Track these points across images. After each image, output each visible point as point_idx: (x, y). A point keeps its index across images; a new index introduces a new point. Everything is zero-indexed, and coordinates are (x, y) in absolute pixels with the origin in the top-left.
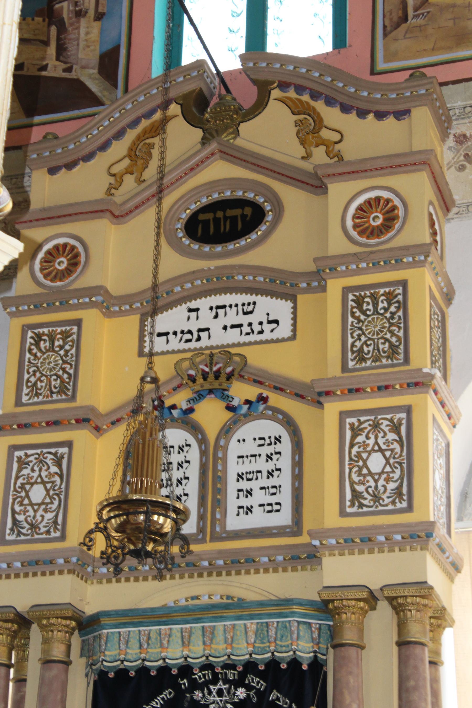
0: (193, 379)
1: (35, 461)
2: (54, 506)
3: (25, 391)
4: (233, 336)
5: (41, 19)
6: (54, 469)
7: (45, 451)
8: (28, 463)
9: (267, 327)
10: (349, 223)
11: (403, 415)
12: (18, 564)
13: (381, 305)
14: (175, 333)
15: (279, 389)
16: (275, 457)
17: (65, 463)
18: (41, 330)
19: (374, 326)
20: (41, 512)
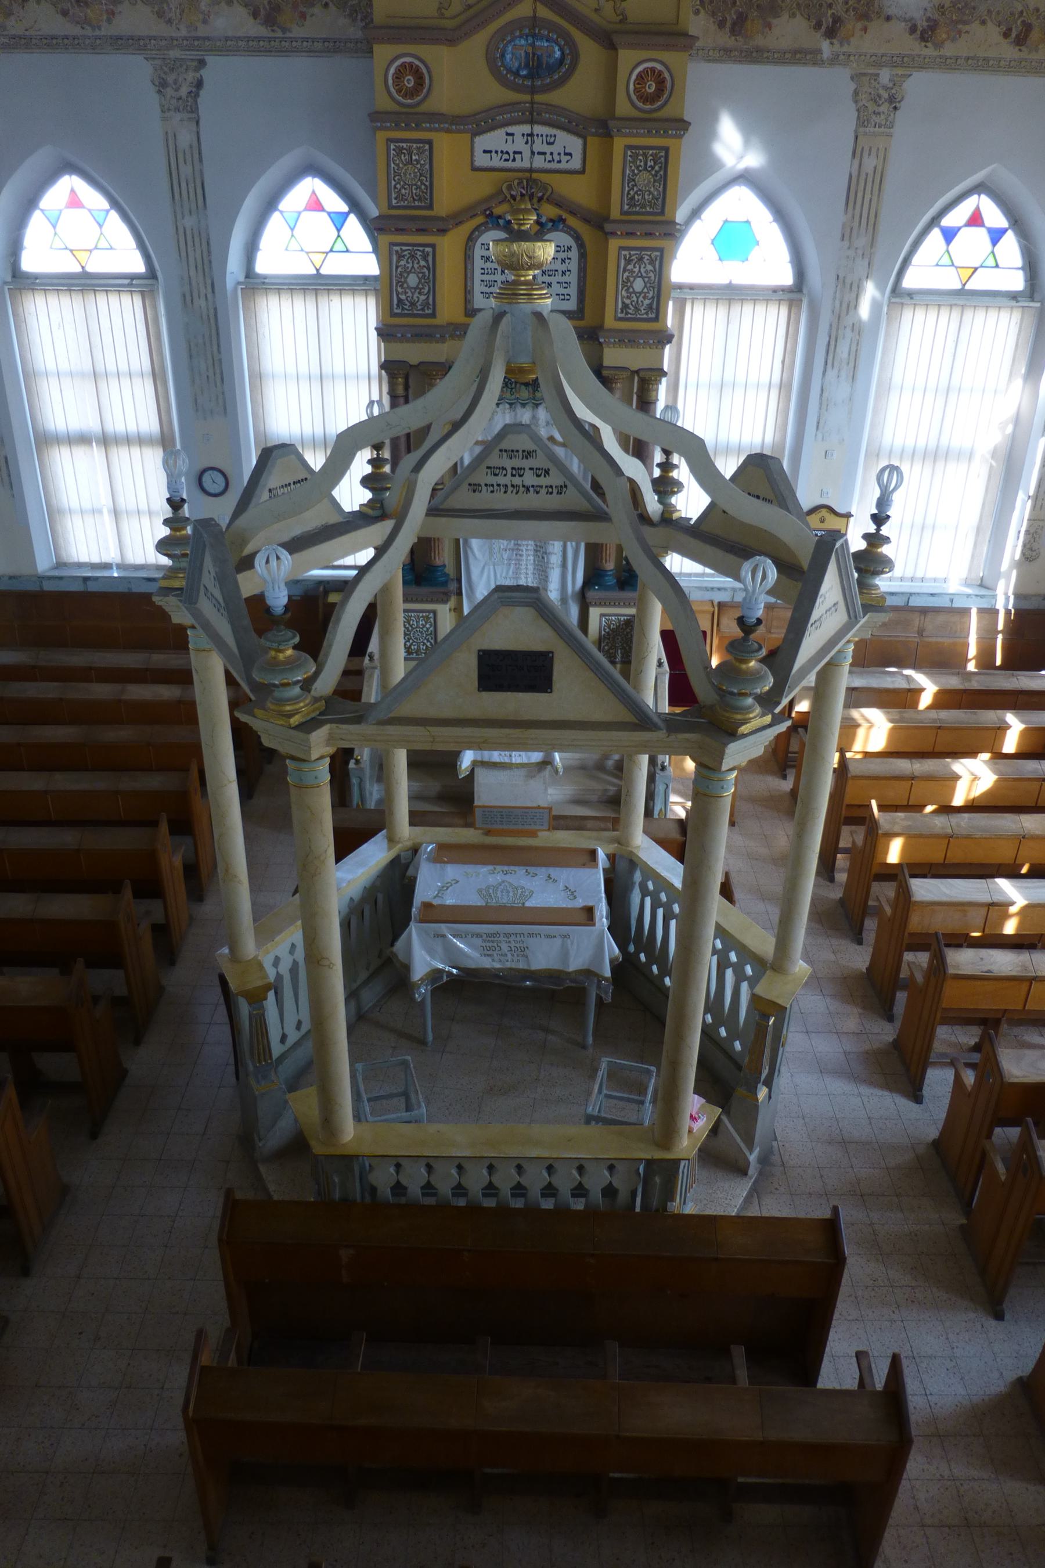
0: (514, 198)
2: (426, 291)
3: (394, 195)
4: (539, 162)
6: (422, 263)
8: (404, 256)
9: (564, 158)
10: (632, 87)
11: (658, 253)
13: (649, 164)
14: (496, 152)
15: (573, 213)
16: (567, 261)
17: (430, 259)
19: (643, 179)
20: (416, 295)
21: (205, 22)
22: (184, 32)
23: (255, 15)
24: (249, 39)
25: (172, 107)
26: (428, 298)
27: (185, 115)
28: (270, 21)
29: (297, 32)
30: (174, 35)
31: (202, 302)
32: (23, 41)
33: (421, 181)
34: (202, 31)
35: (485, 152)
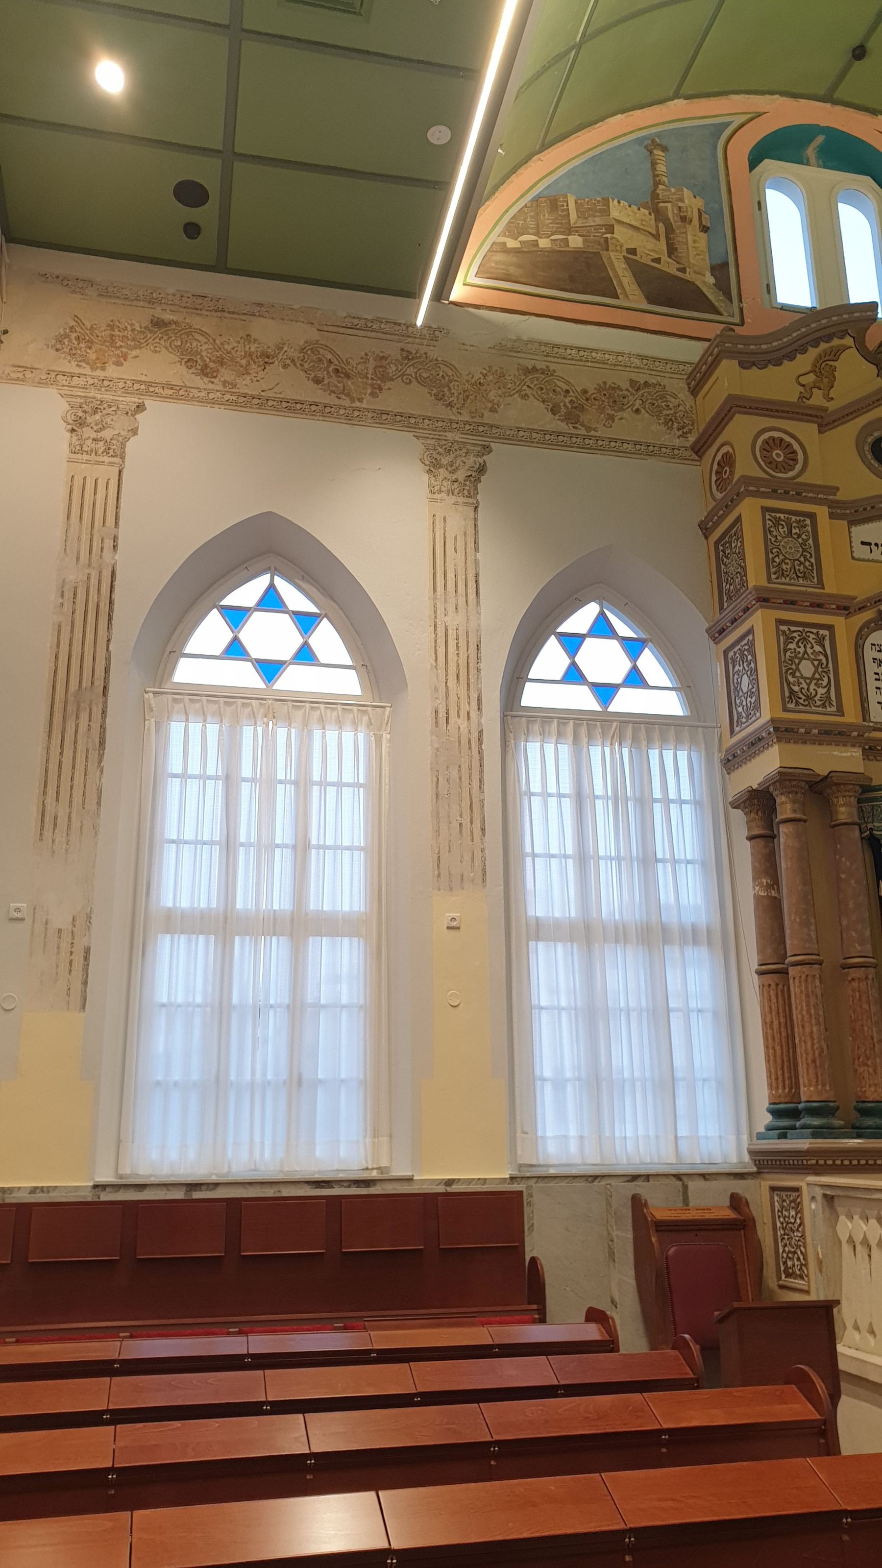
1: (798, 638)
2: (825, 683)
5: (647, 212)
6: (818, 648)
7: (807, 630)
12: (815, 731)
14: (876, 545)
18: (778, 515)
21: (493, 410)
22: (466, 417)
23: (554, 411)
24: (545, 433)
25: (443, 489)
26: (829, 691)
27: (461, 500)
28: (572, 417)
29: (602, 432)
30: (453, 418)
31: (463, 724)
32: (256, 401)
33: (805, 557)
34: (489, 418)
35: (863, 543)
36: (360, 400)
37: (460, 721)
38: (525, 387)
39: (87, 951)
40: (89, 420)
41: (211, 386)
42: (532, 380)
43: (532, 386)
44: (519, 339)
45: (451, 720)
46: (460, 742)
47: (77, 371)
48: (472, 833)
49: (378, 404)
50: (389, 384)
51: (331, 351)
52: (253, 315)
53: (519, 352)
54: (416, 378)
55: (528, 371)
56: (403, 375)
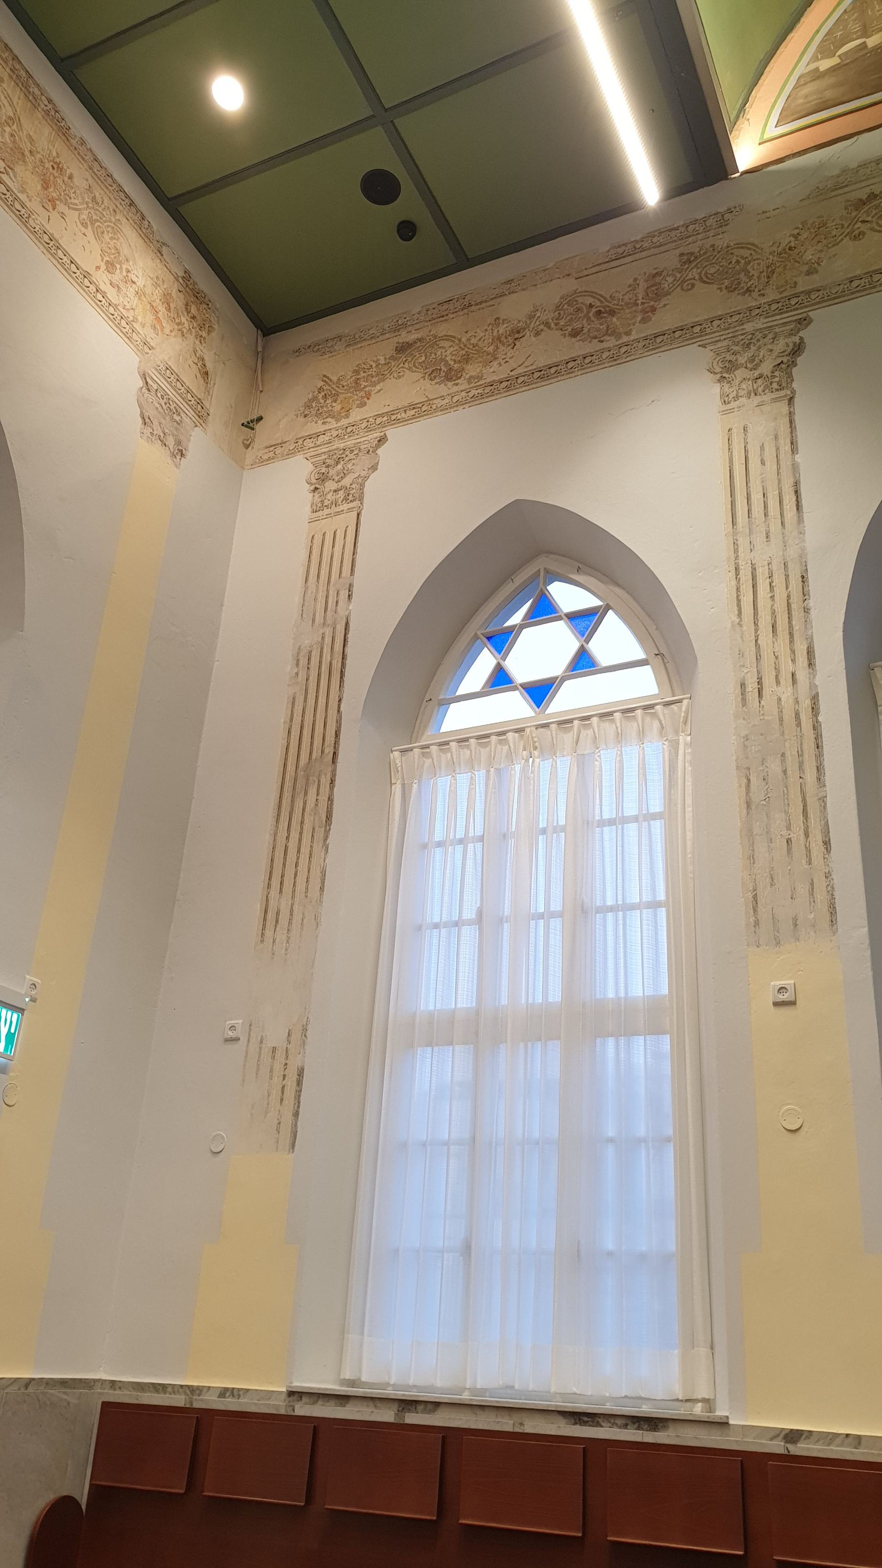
22: (772, 295)
31: (786, 692)
36: (628, 333)
37: (779, 690)
38: (859, 224)
39: (301, 1073)
40: (332, 472)
41: (455, 389)
42: (868, 213)
43: (869, 219)
44: (844, 171)
45: (766, 692)
46: (781, 720)
47: (322, 428)
48: (808, 850)
49: (650, 329)
50: (664, 301)
51: (592, 294)
52: (503, 295)
53: (846, 186)
54: (701, 279)
55: (863, 203)
56: (684, 281)
